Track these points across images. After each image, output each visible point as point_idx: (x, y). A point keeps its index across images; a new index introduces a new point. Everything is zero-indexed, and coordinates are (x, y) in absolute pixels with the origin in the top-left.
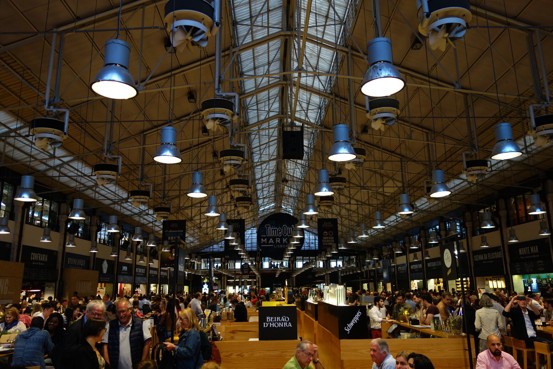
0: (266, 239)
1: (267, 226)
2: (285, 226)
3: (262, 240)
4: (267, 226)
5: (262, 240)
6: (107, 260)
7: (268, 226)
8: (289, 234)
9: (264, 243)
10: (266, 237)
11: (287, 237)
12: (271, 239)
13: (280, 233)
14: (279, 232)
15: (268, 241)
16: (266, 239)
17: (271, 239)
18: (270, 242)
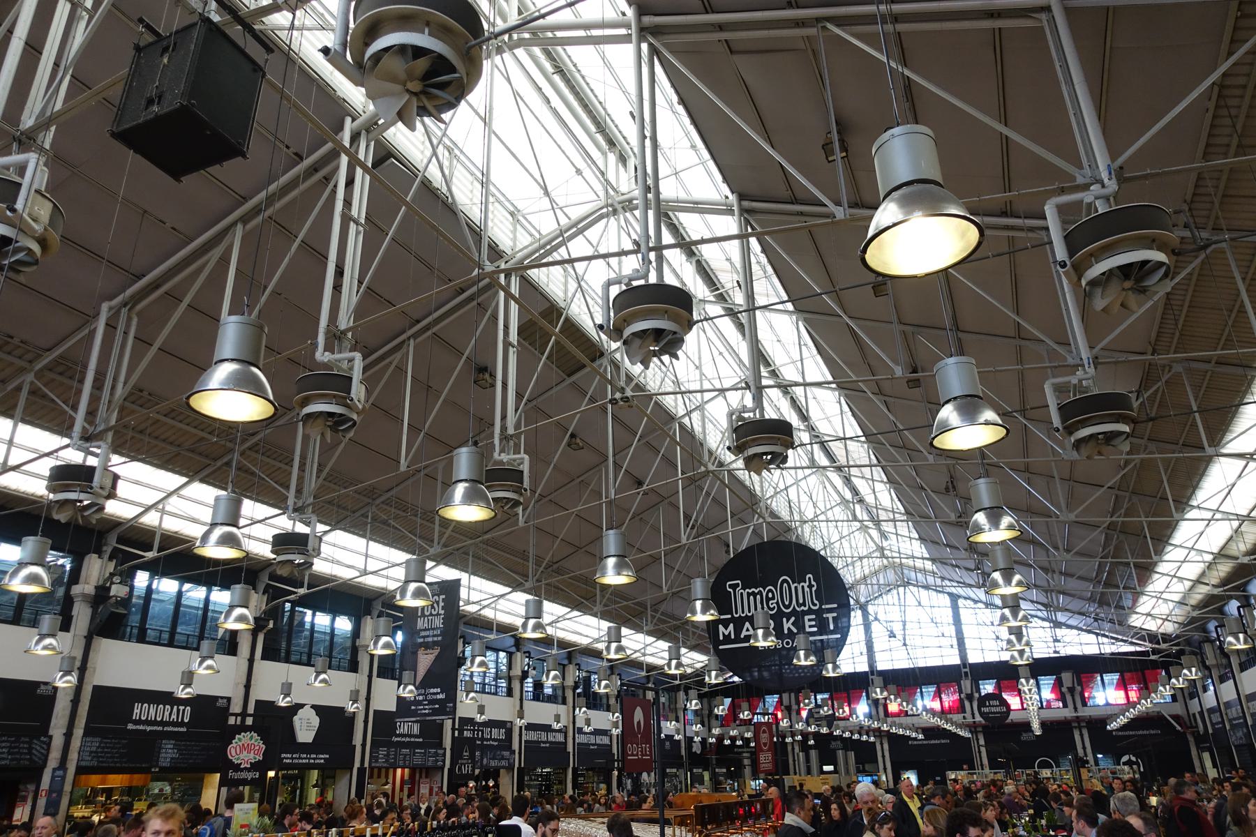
0: (731, 626)
1: (730, 586)
2: (785, 581)
3: (721, 628)
4: (730, 586)
5: (721, 628)
6: (318, 709)
7: (734, 587)
8: (799, 605)
9: (727, 639)
10: (733, 620)
11: (794, 612)
12: (747, 625)
13: (772, 603)
14: (768, 599)
15: (738, 630)
16: (732, 625)
17: (747, 625)
18: (744, 633)
